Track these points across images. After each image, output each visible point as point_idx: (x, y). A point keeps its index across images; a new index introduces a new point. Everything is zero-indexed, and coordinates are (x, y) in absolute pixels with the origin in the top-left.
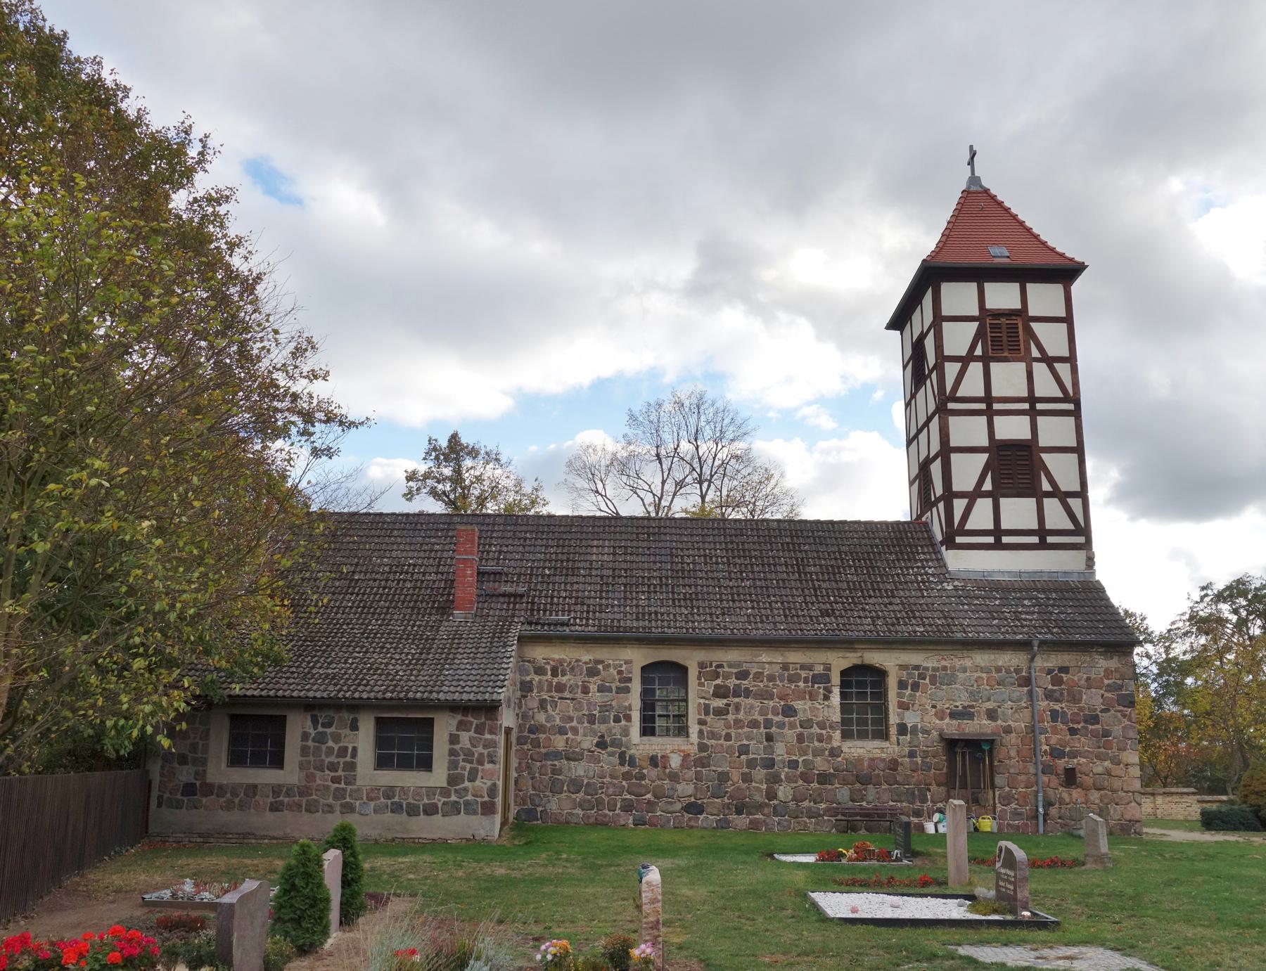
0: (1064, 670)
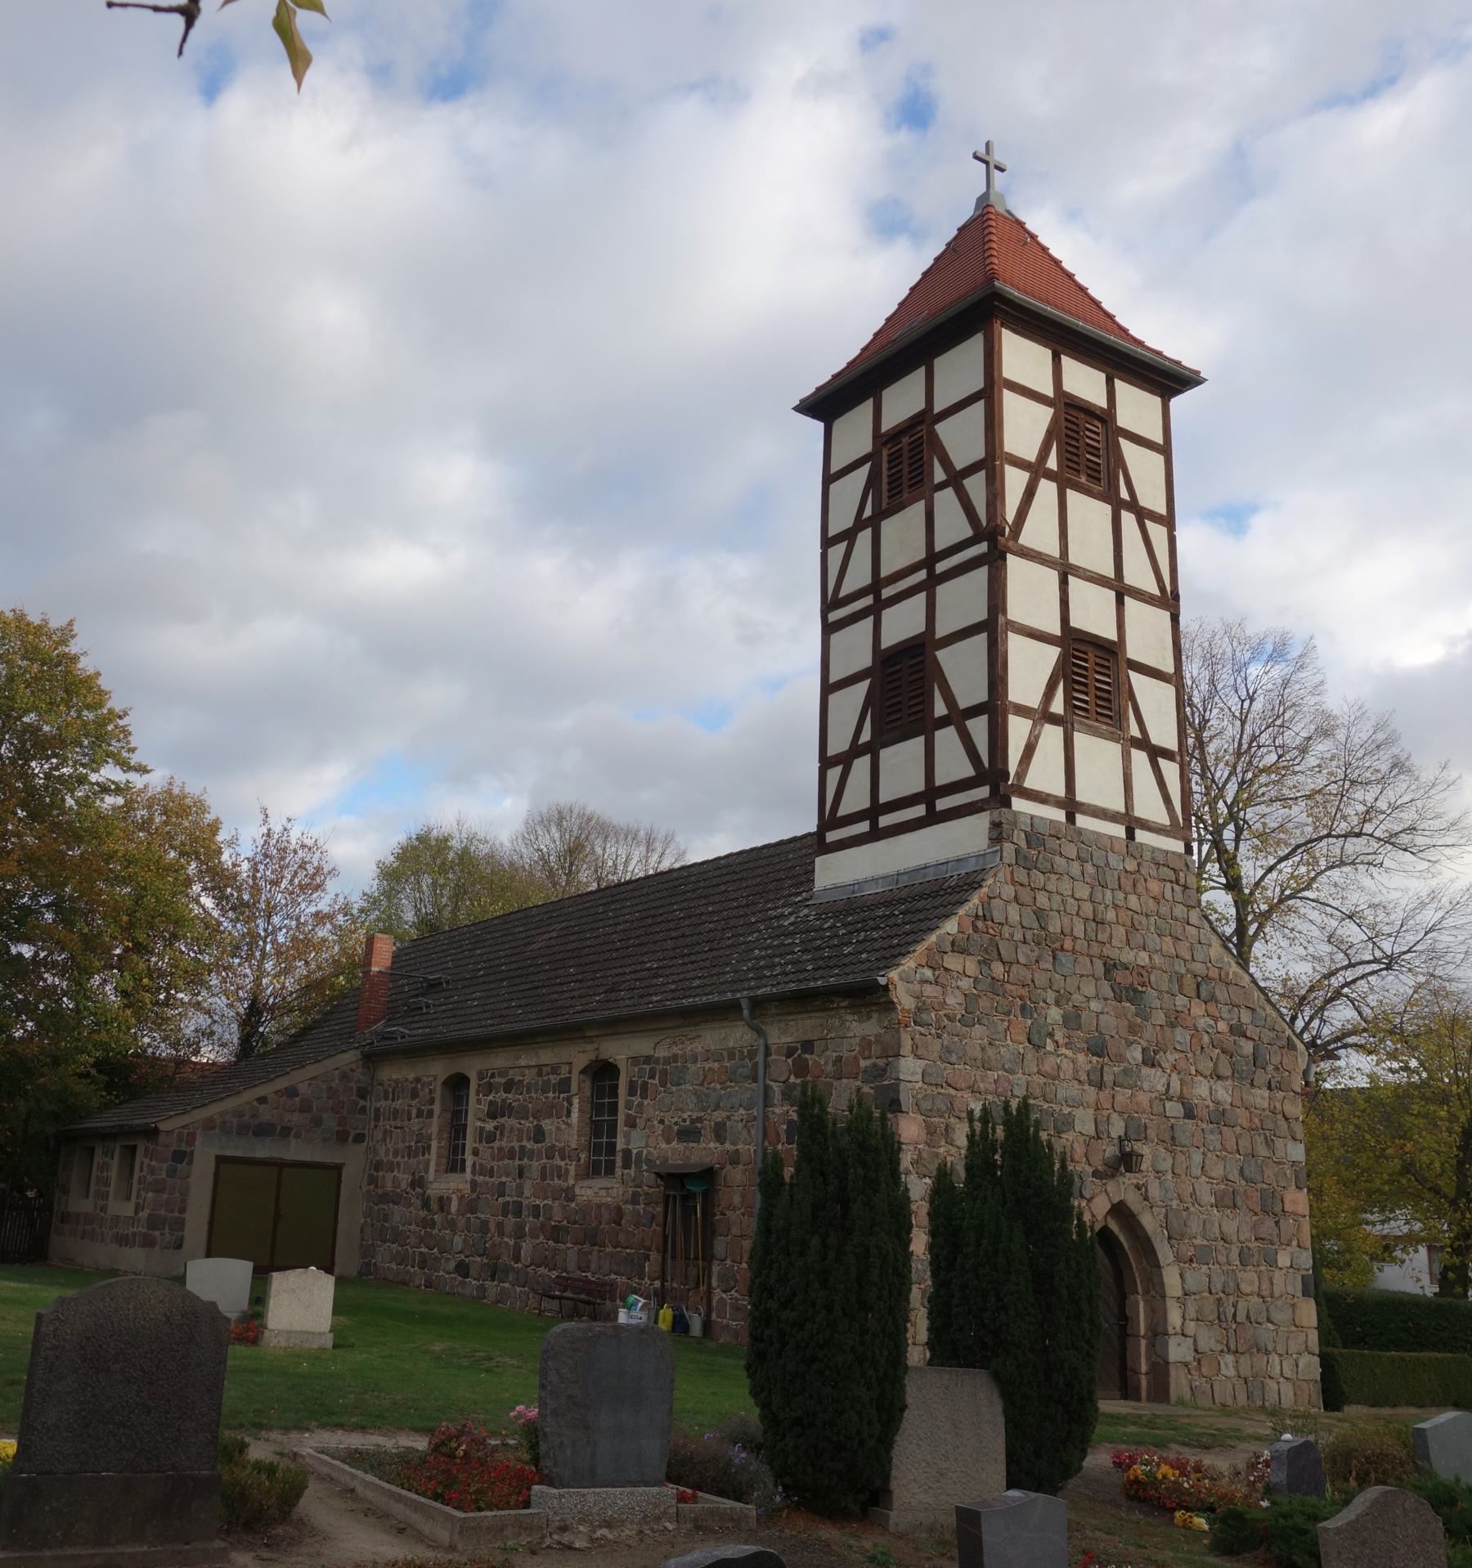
0: (808, 1046)
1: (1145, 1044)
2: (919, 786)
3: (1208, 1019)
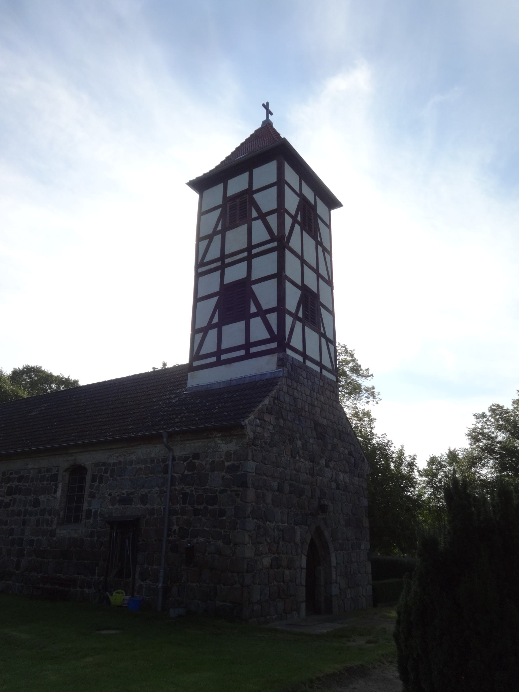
0: (196, 456)
2: (242, 342)
3: (343, 448)
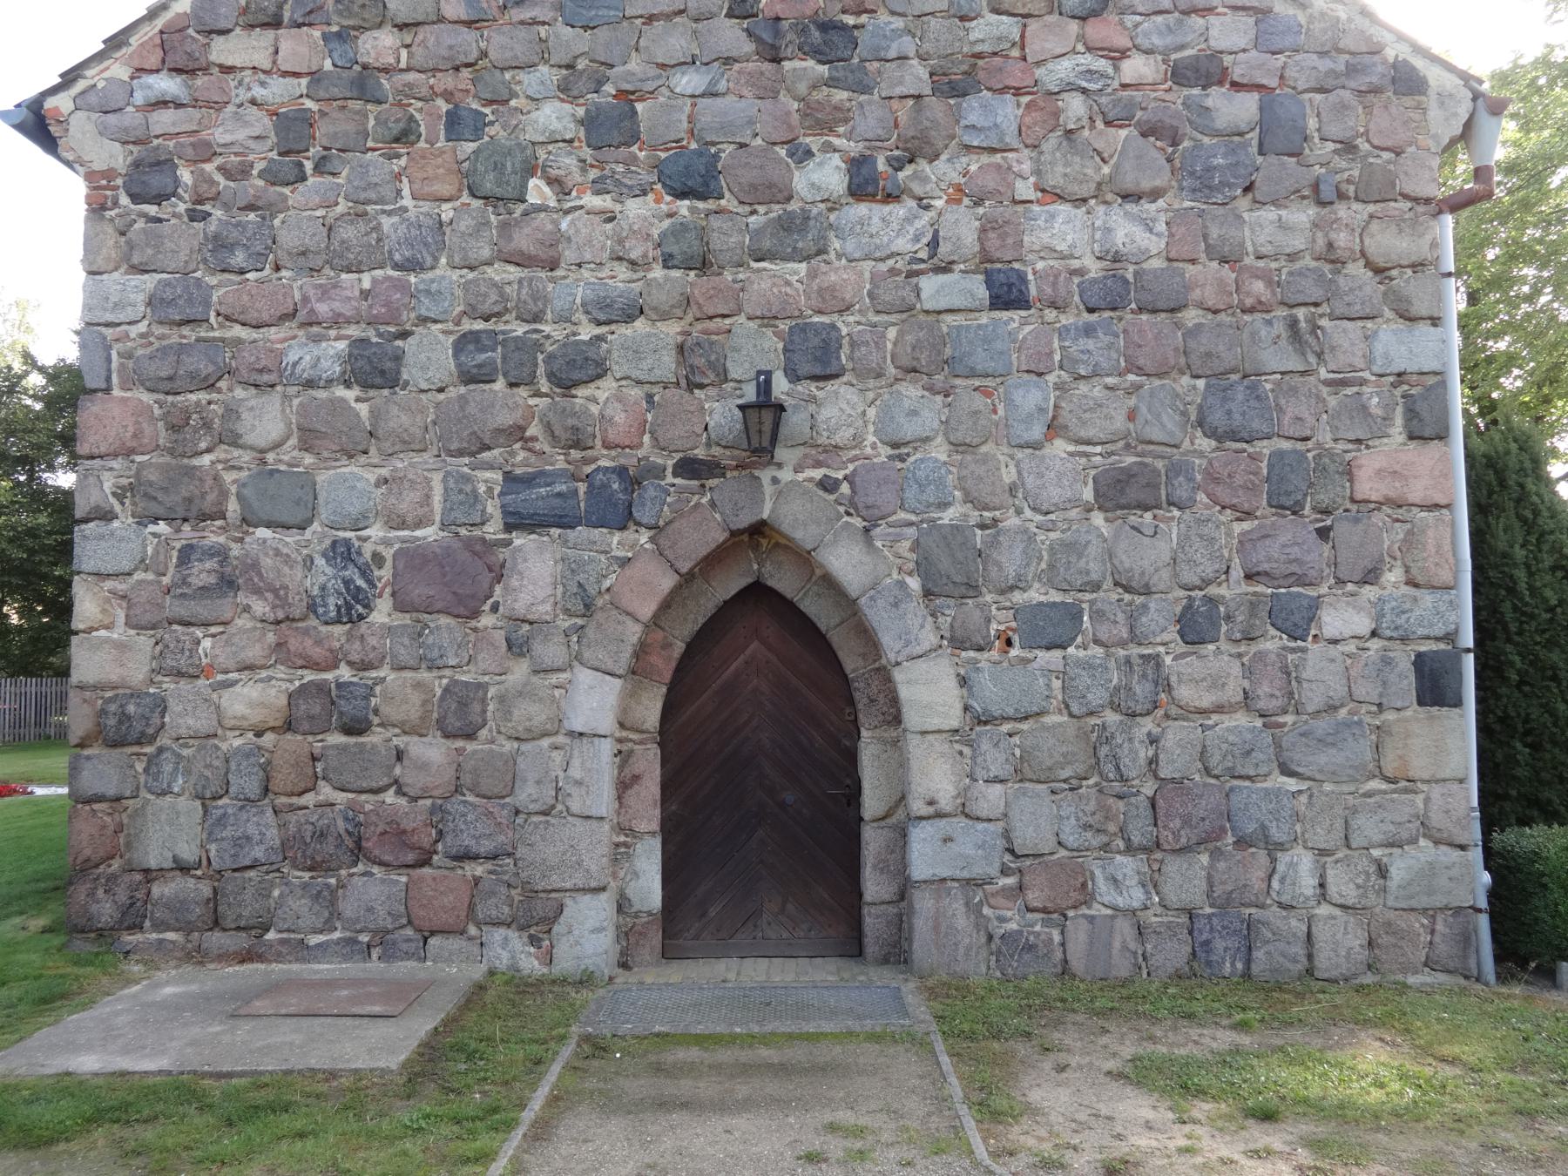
1: (855, 148)
3: (1087, 60)
